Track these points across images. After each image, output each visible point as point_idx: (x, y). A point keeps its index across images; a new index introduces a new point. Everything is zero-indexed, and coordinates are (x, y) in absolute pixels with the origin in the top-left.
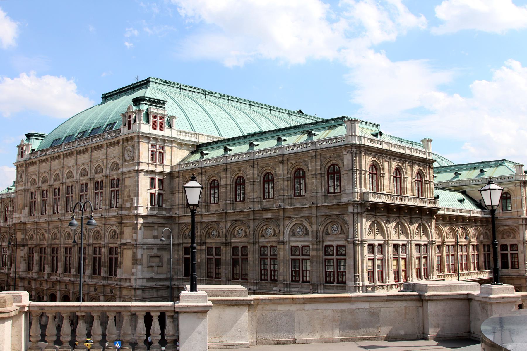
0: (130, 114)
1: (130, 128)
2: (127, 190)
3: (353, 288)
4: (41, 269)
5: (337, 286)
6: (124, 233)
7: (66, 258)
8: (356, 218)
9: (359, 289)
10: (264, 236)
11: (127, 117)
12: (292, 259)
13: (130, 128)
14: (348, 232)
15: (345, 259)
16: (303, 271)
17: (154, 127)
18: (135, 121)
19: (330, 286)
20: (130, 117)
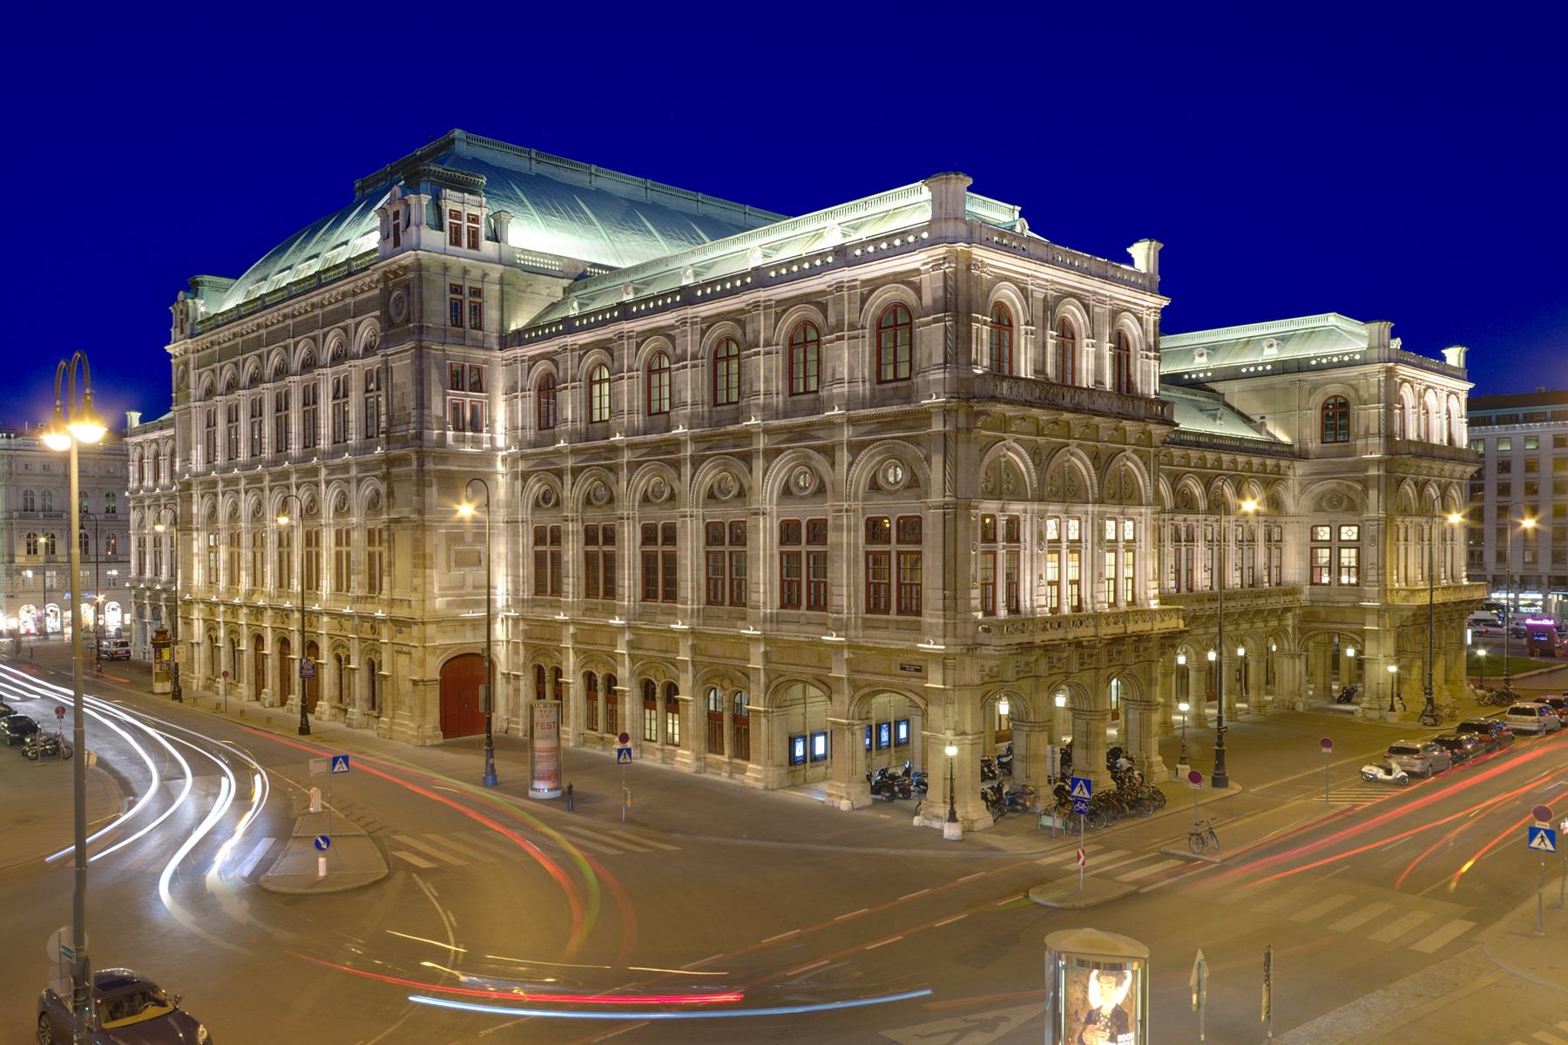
0: (395, 209)
1: (397, 243)
2: (398, 393)
3: (941, 628)
4: (233, 580)
5: (897, 622)
6: (396, 494)
7: (280, 554)
8: (953, 445)
9: (955, 628)
10: (715, 498)
11: (391, 218)
12: (782, 553)
13: (397, 243)
14: (928, 479)
15: (920, 552)
16: (809, 582)
17: (456, 241)
18: (408, 224)
19: (880, 620)
20: (396, 215)
